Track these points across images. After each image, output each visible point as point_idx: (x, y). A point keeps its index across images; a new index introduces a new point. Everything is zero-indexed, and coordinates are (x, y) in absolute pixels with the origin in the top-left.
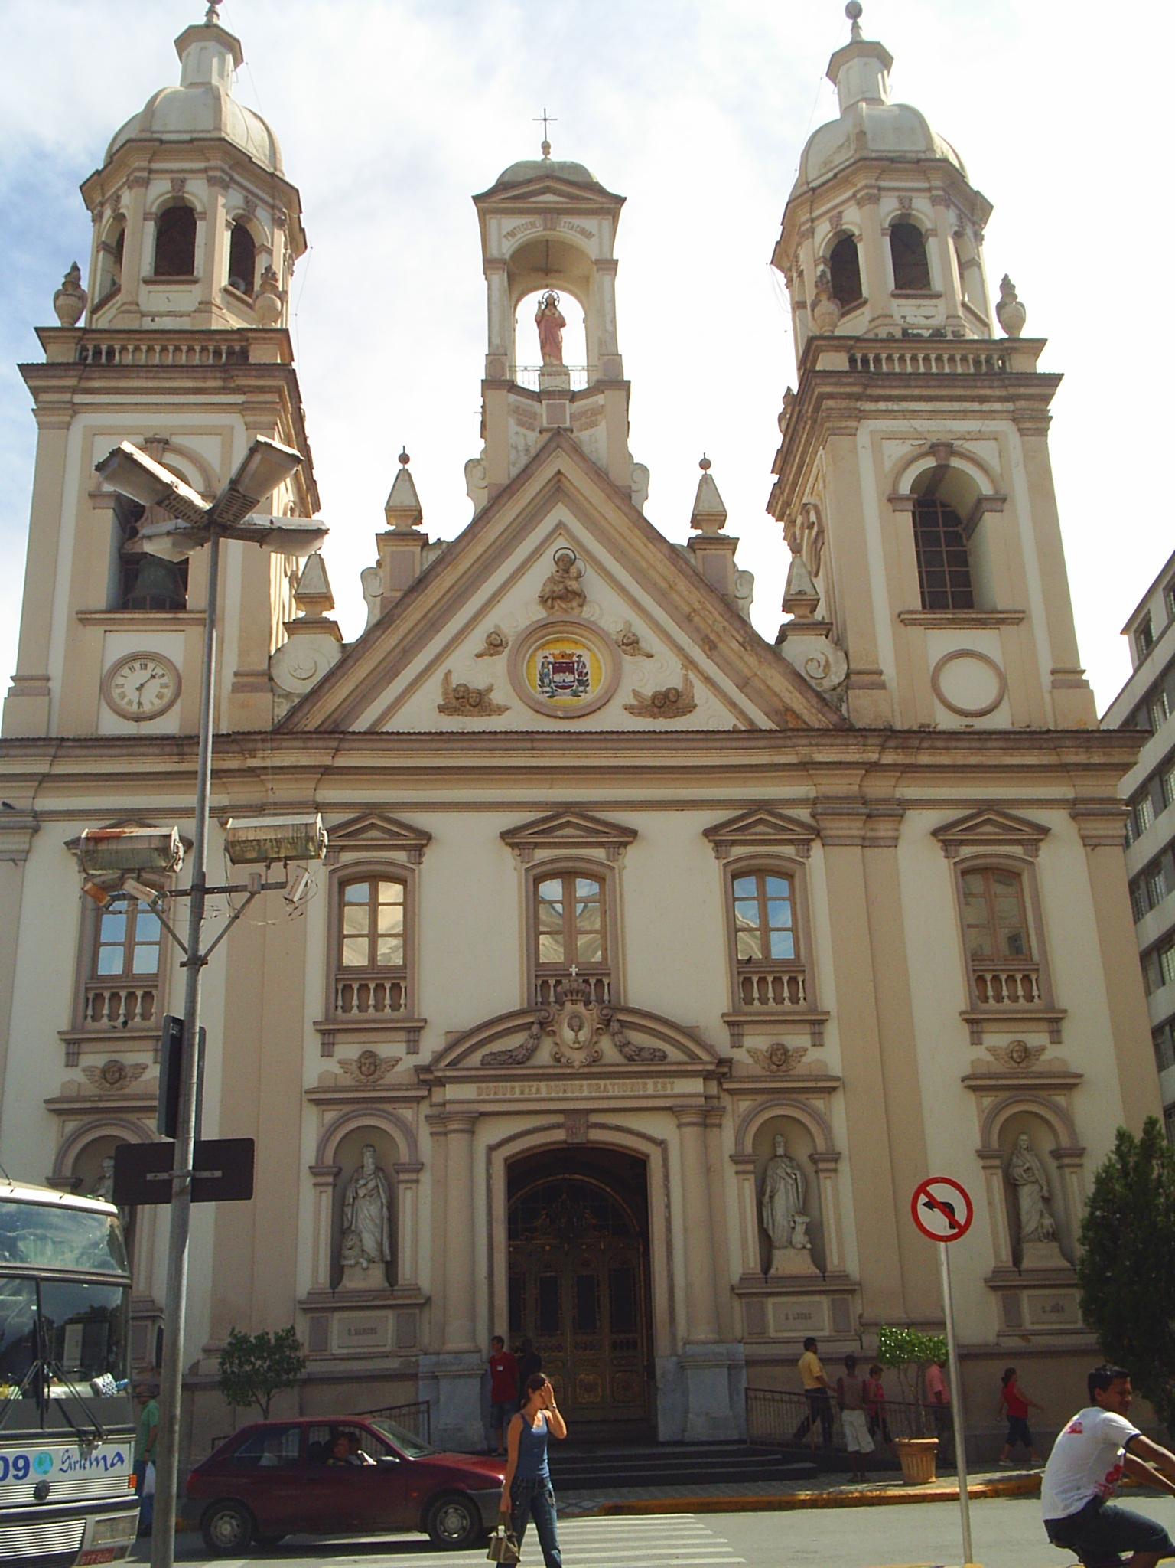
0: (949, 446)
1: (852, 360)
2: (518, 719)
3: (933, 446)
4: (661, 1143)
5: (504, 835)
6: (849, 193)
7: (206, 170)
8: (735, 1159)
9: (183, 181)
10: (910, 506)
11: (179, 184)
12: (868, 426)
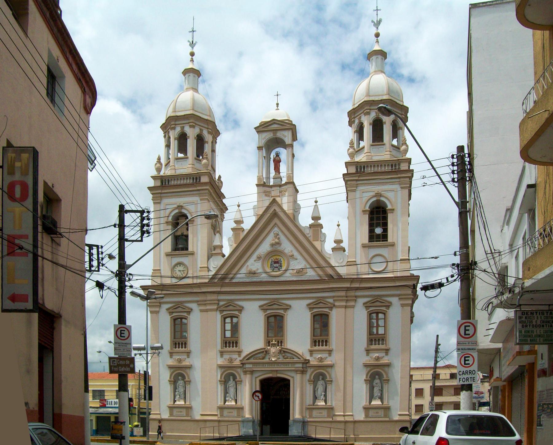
0: (182, 206)
1: (357, 169)
2: (264, 277)
3: (178, 206)
4: (293, 377)
5: (260, 307)
6: (362, 111)
7: (189, 123)
8: (309, 381)
9: (183, 127)
10: (368, 213)
11: (183, 128)
12: (361, 188)
